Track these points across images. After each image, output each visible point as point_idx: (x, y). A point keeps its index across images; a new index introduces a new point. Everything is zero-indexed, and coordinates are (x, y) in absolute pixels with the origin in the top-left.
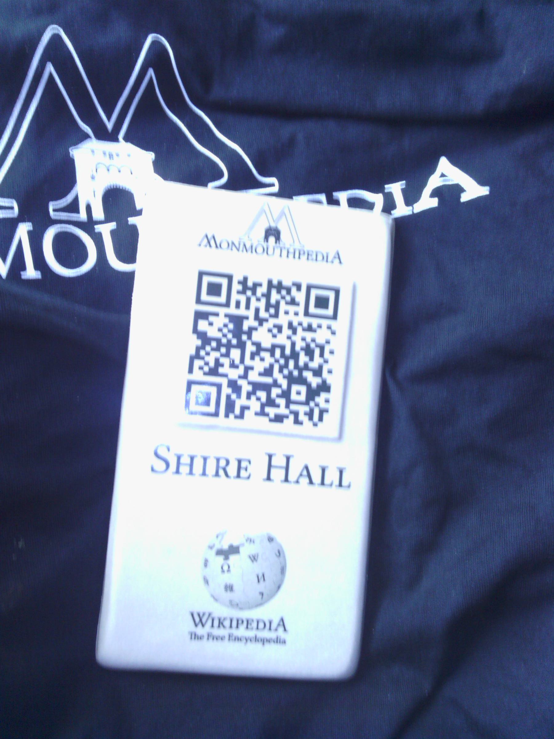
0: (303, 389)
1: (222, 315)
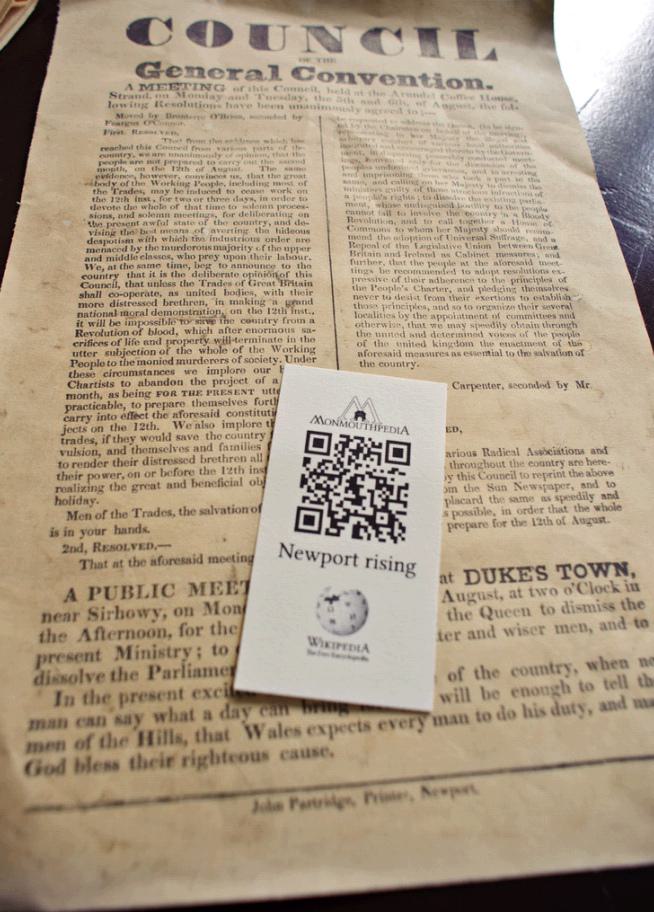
0: (386, 515)
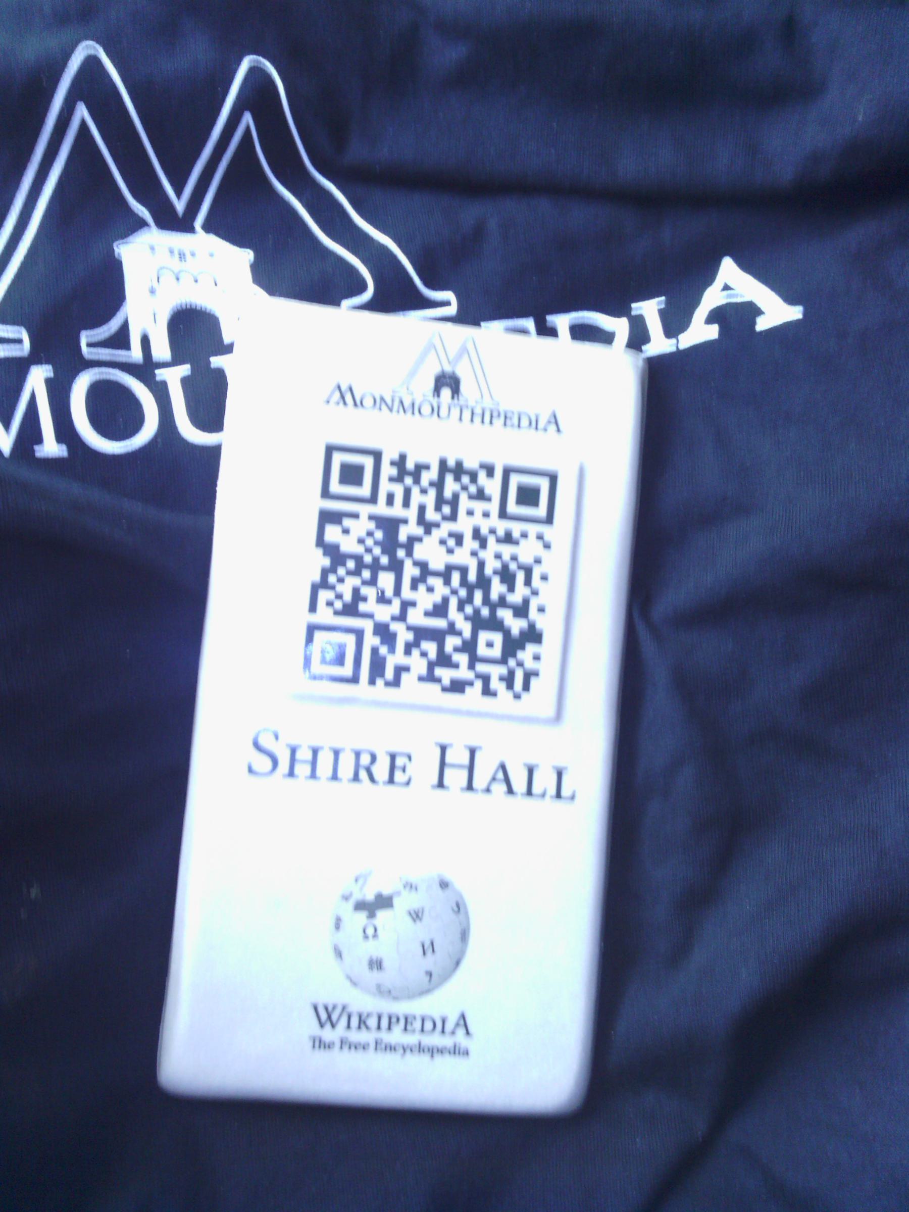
0: (497, 638)
1: (364, 517)
